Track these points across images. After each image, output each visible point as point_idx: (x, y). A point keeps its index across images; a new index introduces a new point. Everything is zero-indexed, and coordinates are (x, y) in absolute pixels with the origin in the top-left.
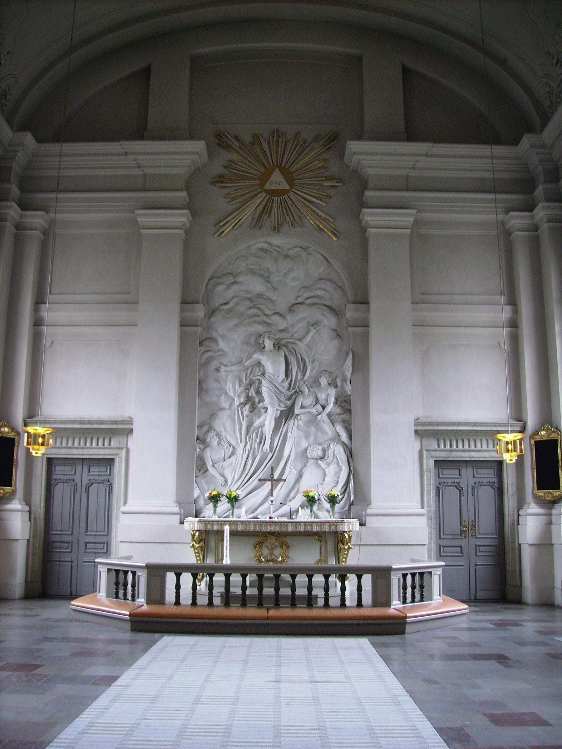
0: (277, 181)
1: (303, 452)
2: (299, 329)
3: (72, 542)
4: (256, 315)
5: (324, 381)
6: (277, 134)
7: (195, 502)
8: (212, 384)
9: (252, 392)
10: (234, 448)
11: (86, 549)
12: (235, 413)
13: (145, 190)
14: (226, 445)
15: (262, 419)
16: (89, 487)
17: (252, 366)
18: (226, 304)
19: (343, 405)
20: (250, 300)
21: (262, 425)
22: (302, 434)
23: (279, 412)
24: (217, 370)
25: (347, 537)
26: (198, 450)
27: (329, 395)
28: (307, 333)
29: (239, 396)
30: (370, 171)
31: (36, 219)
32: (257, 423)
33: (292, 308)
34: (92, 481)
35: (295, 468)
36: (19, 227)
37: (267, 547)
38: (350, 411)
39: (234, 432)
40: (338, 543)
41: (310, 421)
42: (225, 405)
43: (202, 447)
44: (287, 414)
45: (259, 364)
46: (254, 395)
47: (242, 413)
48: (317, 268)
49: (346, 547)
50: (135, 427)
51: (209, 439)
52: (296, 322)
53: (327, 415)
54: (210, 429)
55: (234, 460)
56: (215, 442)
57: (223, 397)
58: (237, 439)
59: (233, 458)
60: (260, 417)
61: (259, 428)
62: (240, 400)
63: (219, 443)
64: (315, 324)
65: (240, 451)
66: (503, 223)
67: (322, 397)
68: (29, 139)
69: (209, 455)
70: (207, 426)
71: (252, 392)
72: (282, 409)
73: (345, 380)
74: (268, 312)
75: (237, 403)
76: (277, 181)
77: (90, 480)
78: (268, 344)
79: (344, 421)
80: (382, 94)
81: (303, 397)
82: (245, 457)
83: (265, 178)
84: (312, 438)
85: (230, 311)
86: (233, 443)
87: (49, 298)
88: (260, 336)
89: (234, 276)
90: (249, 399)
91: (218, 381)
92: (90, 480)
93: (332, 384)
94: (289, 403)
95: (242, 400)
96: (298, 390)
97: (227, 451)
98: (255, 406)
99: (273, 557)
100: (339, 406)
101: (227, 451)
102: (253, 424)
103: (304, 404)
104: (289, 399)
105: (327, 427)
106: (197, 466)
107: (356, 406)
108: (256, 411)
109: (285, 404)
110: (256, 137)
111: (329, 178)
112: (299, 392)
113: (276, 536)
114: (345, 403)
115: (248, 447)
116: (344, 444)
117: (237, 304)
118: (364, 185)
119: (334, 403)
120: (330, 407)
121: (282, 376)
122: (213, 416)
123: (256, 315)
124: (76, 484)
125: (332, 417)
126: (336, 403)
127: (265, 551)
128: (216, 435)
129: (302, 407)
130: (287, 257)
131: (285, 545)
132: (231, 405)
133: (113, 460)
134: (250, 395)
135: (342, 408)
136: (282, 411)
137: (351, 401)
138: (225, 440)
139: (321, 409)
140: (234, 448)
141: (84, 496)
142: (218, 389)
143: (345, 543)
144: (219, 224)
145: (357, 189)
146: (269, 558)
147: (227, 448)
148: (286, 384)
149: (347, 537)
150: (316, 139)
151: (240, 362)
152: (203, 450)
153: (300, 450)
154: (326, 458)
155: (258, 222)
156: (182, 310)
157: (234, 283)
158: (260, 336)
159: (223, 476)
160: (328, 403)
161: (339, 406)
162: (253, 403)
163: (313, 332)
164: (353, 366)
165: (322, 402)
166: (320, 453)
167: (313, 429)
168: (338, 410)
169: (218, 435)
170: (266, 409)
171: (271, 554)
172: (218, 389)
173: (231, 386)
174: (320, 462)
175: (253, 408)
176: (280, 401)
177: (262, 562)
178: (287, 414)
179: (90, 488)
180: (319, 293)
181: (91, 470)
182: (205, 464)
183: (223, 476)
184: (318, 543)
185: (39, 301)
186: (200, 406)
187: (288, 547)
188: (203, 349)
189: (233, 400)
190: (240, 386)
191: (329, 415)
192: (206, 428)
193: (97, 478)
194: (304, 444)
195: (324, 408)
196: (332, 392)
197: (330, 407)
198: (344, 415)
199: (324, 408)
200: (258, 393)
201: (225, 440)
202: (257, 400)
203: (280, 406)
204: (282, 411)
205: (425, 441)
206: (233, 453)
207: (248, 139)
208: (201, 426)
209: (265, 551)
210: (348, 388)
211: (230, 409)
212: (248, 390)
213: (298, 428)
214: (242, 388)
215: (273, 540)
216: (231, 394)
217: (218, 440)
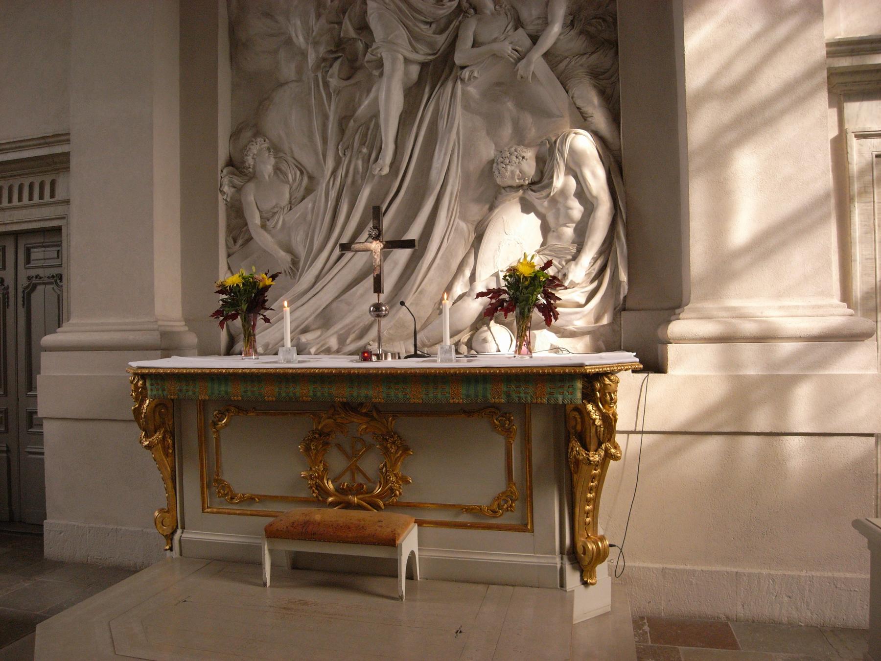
1: (483, 171)
3: (6, 410)
8: (256, 26)
10: (311, 178)
11: (31, 427)
12: (310, 89)
14: (292, 174)
15: (372, 95)
16: (29, 294)
19: (592, 30)
22: (479, 121)
23: (415, 70)
25: (598, 422)
26: (226, 189)
29: (316, 44)
32: (363, 109)
34: (34, 281)
35: (463, 218)
37: (339, 446)
38: (613, 45)
39: (311, 137)
40: (568, 441)
41: (499, 84)
42: (288, 71)
43: (237, 181)
44: (439, 70)
46: (352, 34)
47: (326, 85)
49: (596, 458)
51: (250, 161)
53: (546, 55)
54: (258, 133)
55: (310, 205)
56: (268, 168)
57: (282, 55)
58: (316, 153)
59: (308, 203)
60: (369, 91)
61: (371, 119)
62: (317, 52)
63: (277, 169)
69: (251, 198)
70: (249, 127)
71: (349, 29)
72: (421, 58)
75: (312, 59)
77: (29, 278)
79: (595, 75)
81: (479, 20)
82: (333, 194)
84: (507, 131)
86: (308, 162)
90: (339, 46)
91: (268, 15)
92: (29, 278)
94: (441, 40)
95: (322, 50)
96: (465, 4)
97: (294, 187)
98: (358, 64)
99: (360, 479)
100: (581, 33)
101: (294, 187)
102: (355, 111)
103: (481, 39)
104: (441, 32)
106: (230, 229)
108: (359, 76)
109: (431, 45)
113: (366, 415)
115: (341, 172)
119: (564, 26)
124: (8, 287)
125: (562, 66)
126: (571, 23)
127: (337, 462)
128: (268, 149)
131: (394, 446)
132: (300, 71)
133: (58, 230)
134: (342, 35)
135: (591, 37)
136: (424, 65)
137: (615, 20)
138: (290, 159)
139: (528, 42)
140: (311, 178)
141: (22, 312)
142: (272, 35)
143: (593, 447)
146: (346, 482)
147: (294, 180)
149: (598, 422)
152: (239, 189)
153: (475, 166)
154: (545, 182)
159: (289, 250)
160: (546, 22)
161: (581, 33)
162: (351, 57)
165: (531, 28)
166: (529, 167)
167: (510, 105)
168: (578, 44)
170: (380, 64)
171: (354, 470)
172: (272, 35)
173: (299, 23)
174: (532, 196)
175: (353, 67)
176: (415, 37)
177: (328, 494)
178: (439, 70)
179: (33, 295)
181: (33, 257)
182: (246, 224)
183: (289, 250)
184: (500, 440)
186: (235, 87)
187: (406, 449)
189: (304, 54)
190: (318, 16)
192: (248, 134)
193: (40, 272)
194: (487, 151)
195: (535, 39)
198: (594, 56)
200: (364, 28)
201: (290, 159)
202: (360, 46)
203: (415, 50)
204: (424, 65)
205: (852, 108)
206: (309, 191)
208: (235, 135)
209: (337, 462)
211: (300, 80)
212: (340, 23)
213: (466, 107)
214: (323, 20)
215: (359, 426)
216: (300, 40)
217: (272, 161)
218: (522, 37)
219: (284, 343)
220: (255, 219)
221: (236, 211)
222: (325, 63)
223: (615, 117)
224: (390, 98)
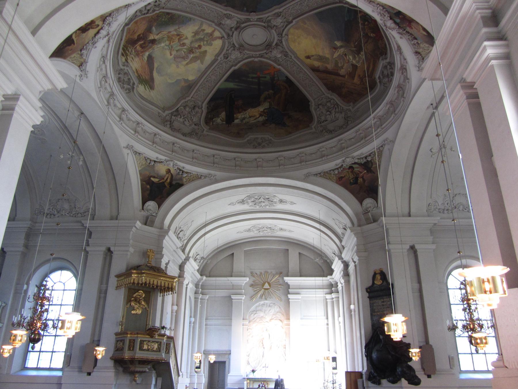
0: (267, 286)
6: (266, 272)
13: (233, 289)
48: (278, 310)
68: (204, 278)
76: (267, 286)
80: (294, 261)
83: (263, 285)
89: (257, 311)
110: (261, 273)
111: (280, 285)
118: (288, 286)
130: (269, 306)
144: (252, 297)
145: (287, 289)
150: (277, 274)
155: (261, 297)
207: (258, 273)
219: (257, 375)
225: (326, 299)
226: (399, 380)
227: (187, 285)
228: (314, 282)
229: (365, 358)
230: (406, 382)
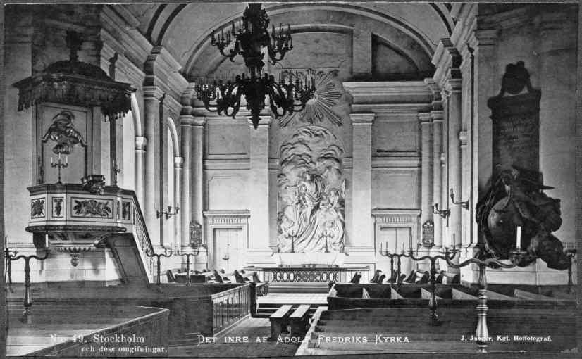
2: (322, 168)
4: (302, 163)
5: (332, 193)
7: (278, 246)
9: (301, 198)
17: (301, 187)
18: (289, 158)
20: (300, 156)
21: (305, 213)
24: (286, 188)
27: (334, 199)
28: (325, 170)
30: (354, 95)
31: (200, 120)
32: (303, 212)
33: (319, 159)
36: (193, 124)
44: (316, 208)
45: (304, 185)
50: (251, 214)
52: (319, 166)
56: (285, 220)
64: (328, 167)
65: (296, 224)
66: (418, 117)
67: (332, 200)
71: (301, 198)
73: (342, 192)
74: (308, 161)
75: (295, 203)
78: (308, 177)
79: (341, 210)
85: (291, 160)
87: (209, 157)
88: (304, 173)
90: (300, 201)
93: (336, 194)
105: (334, 212)
107: (347, 202)
112: (321, 198)
114: (342, 202)
116: (341, 220)
117: (294, 158)
120: (336, 205)
121: (314, 191)
122: (284, 210)
123: (302, 163)
129: (323, 205)
130: (316, 135)
135: (340, 204)
148: (316, 195)
151: (296, 186)
156: (269, 162)
157: (293, 148)
158: (304, 173)
163: (327, 170)
164: (345, 186)
168: (338, 206)
169: (287, 217)
170: (307, 206)
175: (302, 206)
178: (316, 208)
180: (331, 152)
185: (204, 159)
188: (279, 179)
191: (335, 208)
195: (332, 205)
196: (337, 198)
197: (335, 205)
199: (332, 205)
200: (304, 198)
208: (279, 213)
210: (343, 196)
218: (330, 205)
220: (283, 229)
221: (279, 227)
222: (297, 204)
223: (344, 217)
224: (308, 211)
225: (420, 121)
226: (533, 261)
227: (161, 99)
228: (398, 90)
229: (476, 225)
230: (545, 264)
